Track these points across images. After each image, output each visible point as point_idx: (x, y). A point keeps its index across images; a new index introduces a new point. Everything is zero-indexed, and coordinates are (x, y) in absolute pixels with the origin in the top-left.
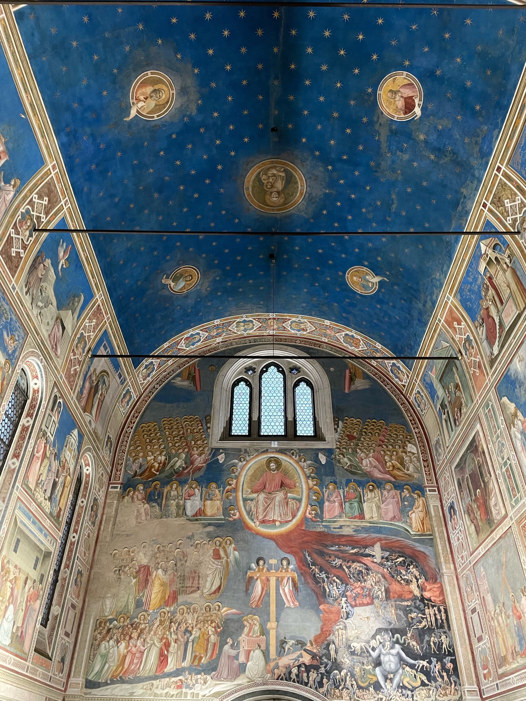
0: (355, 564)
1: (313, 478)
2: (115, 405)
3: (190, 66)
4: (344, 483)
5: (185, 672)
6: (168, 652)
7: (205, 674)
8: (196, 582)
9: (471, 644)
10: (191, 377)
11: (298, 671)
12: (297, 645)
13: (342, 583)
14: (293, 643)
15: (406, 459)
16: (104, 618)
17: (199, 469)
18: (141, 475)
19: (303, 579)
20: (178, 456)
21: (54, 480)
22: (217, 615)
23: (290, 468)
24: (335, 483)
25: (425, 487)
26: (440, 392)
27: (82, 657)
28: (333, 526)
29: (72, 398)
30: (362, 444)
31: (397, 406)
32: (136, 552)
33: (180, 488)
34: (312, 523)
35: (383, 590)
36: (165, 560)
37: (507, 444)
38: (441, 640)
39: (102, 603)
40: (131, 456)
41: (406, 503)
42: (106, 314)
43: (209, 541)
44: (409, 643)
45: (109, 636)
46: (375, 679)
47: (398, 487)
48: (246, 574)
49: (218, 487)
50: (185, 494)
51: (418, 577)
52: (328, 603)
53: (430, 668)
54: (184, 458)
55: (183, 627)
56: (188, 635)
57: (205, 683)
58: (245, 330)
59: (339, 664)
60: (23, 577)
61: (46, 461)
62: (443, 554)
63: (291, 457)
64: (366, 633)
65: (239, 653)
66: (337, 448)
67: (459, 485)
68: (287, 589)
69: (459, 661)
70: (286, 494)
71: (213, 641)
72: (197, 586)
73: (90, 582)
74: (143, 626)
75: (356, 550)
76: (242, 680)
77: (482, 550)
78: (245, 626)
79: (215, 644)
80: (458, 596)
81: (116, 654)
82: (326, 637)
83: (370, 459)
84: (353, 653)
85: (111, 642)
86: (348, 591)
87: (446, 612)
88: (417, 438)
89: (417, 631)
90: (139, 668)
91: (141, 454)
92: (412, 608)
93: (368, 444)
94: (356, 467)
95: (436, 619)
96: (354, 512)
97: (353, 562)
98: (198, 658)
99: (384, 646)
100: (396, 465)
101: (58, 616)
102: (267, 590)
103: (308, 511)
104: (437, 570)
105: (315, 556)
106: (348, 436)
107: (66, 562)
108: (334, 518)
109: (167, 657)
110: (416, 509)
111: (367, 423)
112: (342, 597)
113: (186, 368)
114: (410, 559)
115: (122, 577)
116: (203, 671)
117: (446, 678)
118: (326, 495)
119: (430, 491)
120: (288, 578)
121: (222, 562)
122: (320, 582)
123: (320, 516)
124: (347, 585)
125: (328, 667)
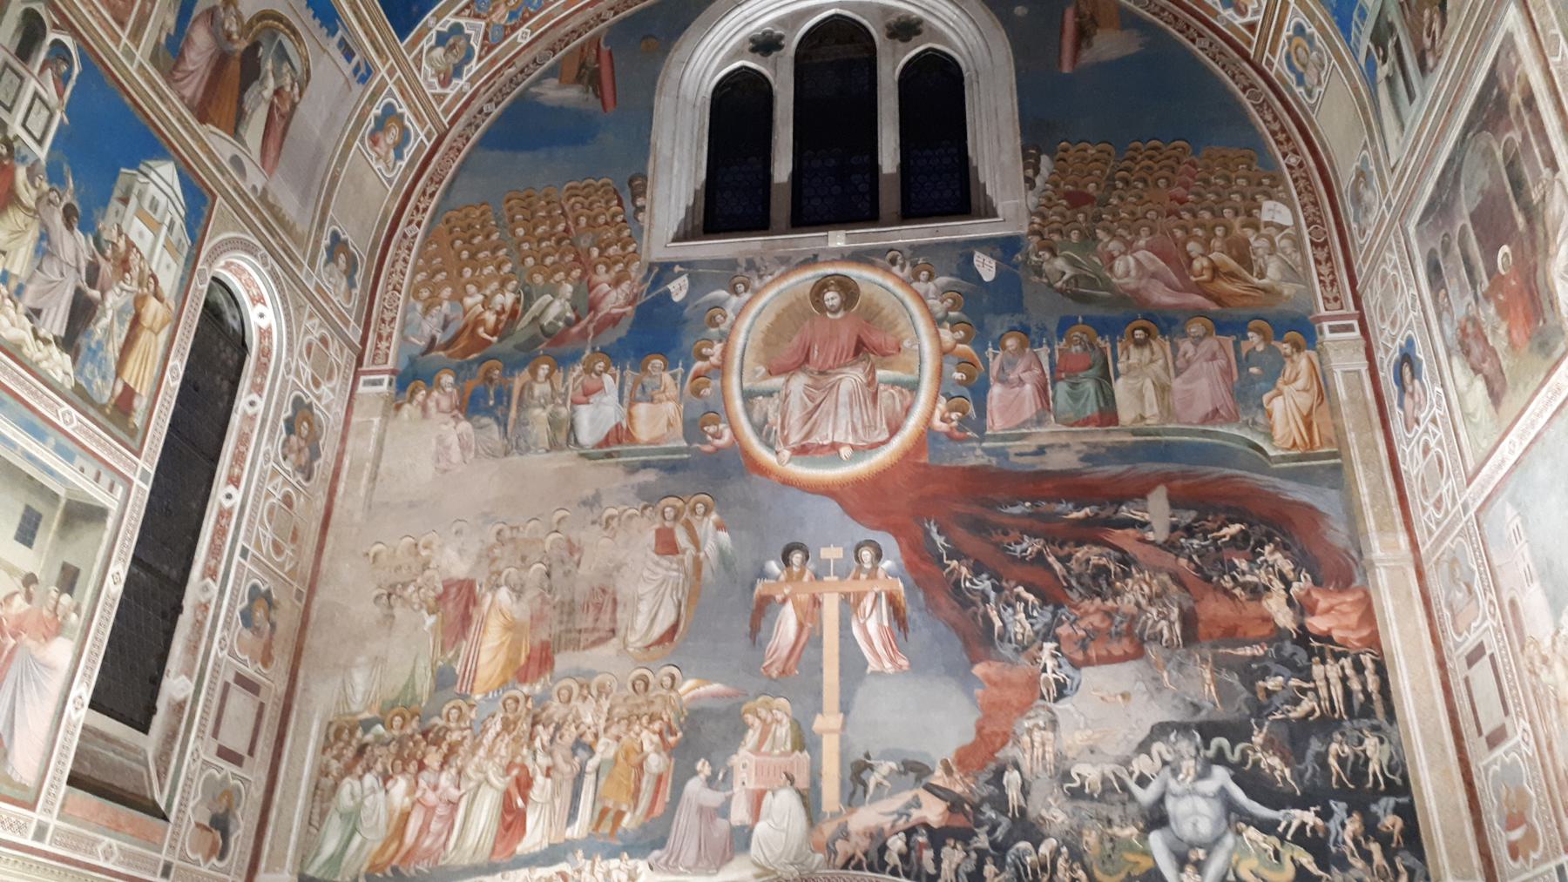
0: (1086, 548)
1: (954, 324)
2: (348, 146)
4: (1053, 327)
5: (574, 852)
6: (525, 799)
7: (631, 857)
8: (605, 618)
10: (587, 73)
11: (907, 844)
12: (905, 773)
13: (1044, 602)
14: (892, 770)
15: (1258, 244)
16: (348, 718)
17: (614, 320)
18: (448, 345)
19: (921, 595)
21: (78, 292)
23: (883, 302)
24: (1025, 330)
25: (1320, 319)
27: (291, 819)
28: (1017, 451)
31: (1232, 95)
32: (434, 547)
34: (952, 444)
35: (1175, 613)
36: (519, 563)
38: (1364, 751)
39: (343, 681)
40: (417, 298)
41: (1254, 370)
43: (645, 508)
44: (1256, 763)
45: (363, 763)
46: (1146, 864)
47: (1228, 326)
48: (753, 586)
49: (670, 365)
50: (574, 390)
51: (1291, 576)
52: (1001, 658)
53: (1327, 831)
54: (569, 295)
55: (570, 734)
56: (582, 754)
59: (1033, 825)
62: (1373, 506)
63: (887, 271)
64: (1120, 737)
65: (729, 799)
67: (1434, 271)
68: (873, 625)
69: (1424, 809)
70: (873, 371)
71: (655, 770)
72: (607, 627)
73: (311, 627)
74: (455, 736)
75: (1087, 510)
77: (1509, 451)
78: (746, 727)
79: (660, 779)
80: (1422, 622)
81: (382, 810)
82: (992, 754)
83: (1140, 255)
85: (369, 779)
86: (1061, 622)
87: (1381, 670)
88: (1295, 181)
89: (1284, 730)
90: (445, 845)
91: (447, 292)
92: (1270, 664)
93: (1132, 213)
94: (1092, 282)
95: (1348, 693)
96: (1084, 406)
98: (611, 814)
99: (1175, 772)
100: (1226, 264)
101: (185, 701)
102: (812, 630)
103: (937, 414)
104: (1354, 554)
105: (961, 534)
106: (1067, 196)
107: (207, 561)
108: (1018, 427)
109: (521, 816)
110: (1286, 383)
111: (1131, 153)
112: (1045, 639)
114: (1264, 528)
115: (398, 612)
116: (626, 848)
118: (994, 367)
119: (1333, 330)
120: (878, 596)
121: (683, 561)
122: (973, 603)
123: (975, 422)
124: (1058, 606)
125: (1000, 834)
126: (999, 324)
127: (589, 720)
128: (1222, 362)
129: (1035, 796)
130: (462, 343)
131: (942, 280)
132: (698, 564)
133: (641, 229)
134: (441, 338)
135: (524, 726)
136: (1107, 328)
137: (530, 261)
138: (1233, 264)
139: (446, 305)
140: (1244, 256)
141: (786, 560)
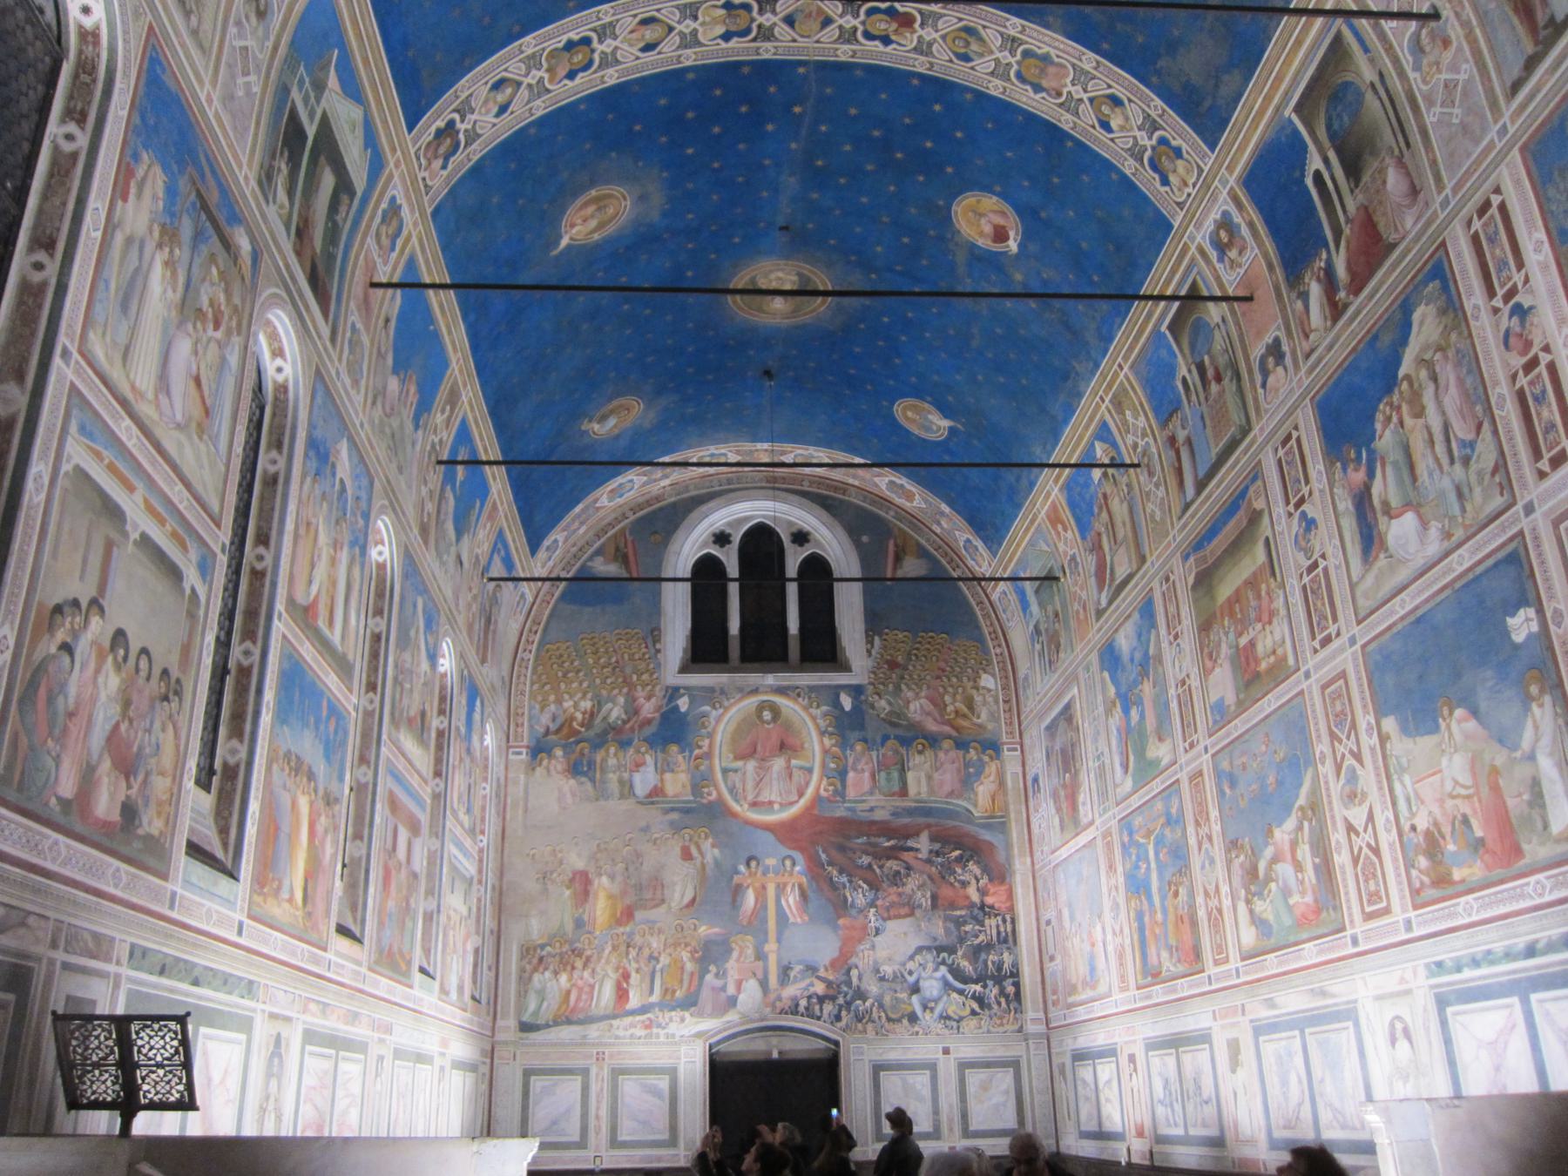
1: (831, 734)
4: (879, 740)
8: (659, 892)
10: (624, 559)
15: (978, 699)
17: (649, 722)
18: (558, 731)
20: (613, 700)
24: (865, 741)
26: (1034, 608)
29: (473, 658)
33: (621, 754)
37: (1103, 736)
46: (909, 1009)
47: (961, 745)
49: (682, 751)
55: (646, 952)
57: (683, 1020)
68: (791, 900)
70: (789, 761)
74: (588, 953)
76: (732, 1016)
79: (692, 974)
85: (548, 974)
87: (1013, 921)
94: (899, 716)
95: (999, 933)
97: (888, 858)
105: (834, 853)
106: (887, 662)
109: (626, 992)
115: (550, 887)
117: (1004, 1005)
118: (850, 760)
123: (841, 793)
126: (855, 735)
127: (655, 945)
129: (864, 979)
130: (565, 731)
131: (825, 708)
132: (703, 866)
133: (659, 665)
134: (553, 727)
135: (623, 948)
136: (906, 742)
137: (598, 681)
138: (965, 710)
139: (553, 707)
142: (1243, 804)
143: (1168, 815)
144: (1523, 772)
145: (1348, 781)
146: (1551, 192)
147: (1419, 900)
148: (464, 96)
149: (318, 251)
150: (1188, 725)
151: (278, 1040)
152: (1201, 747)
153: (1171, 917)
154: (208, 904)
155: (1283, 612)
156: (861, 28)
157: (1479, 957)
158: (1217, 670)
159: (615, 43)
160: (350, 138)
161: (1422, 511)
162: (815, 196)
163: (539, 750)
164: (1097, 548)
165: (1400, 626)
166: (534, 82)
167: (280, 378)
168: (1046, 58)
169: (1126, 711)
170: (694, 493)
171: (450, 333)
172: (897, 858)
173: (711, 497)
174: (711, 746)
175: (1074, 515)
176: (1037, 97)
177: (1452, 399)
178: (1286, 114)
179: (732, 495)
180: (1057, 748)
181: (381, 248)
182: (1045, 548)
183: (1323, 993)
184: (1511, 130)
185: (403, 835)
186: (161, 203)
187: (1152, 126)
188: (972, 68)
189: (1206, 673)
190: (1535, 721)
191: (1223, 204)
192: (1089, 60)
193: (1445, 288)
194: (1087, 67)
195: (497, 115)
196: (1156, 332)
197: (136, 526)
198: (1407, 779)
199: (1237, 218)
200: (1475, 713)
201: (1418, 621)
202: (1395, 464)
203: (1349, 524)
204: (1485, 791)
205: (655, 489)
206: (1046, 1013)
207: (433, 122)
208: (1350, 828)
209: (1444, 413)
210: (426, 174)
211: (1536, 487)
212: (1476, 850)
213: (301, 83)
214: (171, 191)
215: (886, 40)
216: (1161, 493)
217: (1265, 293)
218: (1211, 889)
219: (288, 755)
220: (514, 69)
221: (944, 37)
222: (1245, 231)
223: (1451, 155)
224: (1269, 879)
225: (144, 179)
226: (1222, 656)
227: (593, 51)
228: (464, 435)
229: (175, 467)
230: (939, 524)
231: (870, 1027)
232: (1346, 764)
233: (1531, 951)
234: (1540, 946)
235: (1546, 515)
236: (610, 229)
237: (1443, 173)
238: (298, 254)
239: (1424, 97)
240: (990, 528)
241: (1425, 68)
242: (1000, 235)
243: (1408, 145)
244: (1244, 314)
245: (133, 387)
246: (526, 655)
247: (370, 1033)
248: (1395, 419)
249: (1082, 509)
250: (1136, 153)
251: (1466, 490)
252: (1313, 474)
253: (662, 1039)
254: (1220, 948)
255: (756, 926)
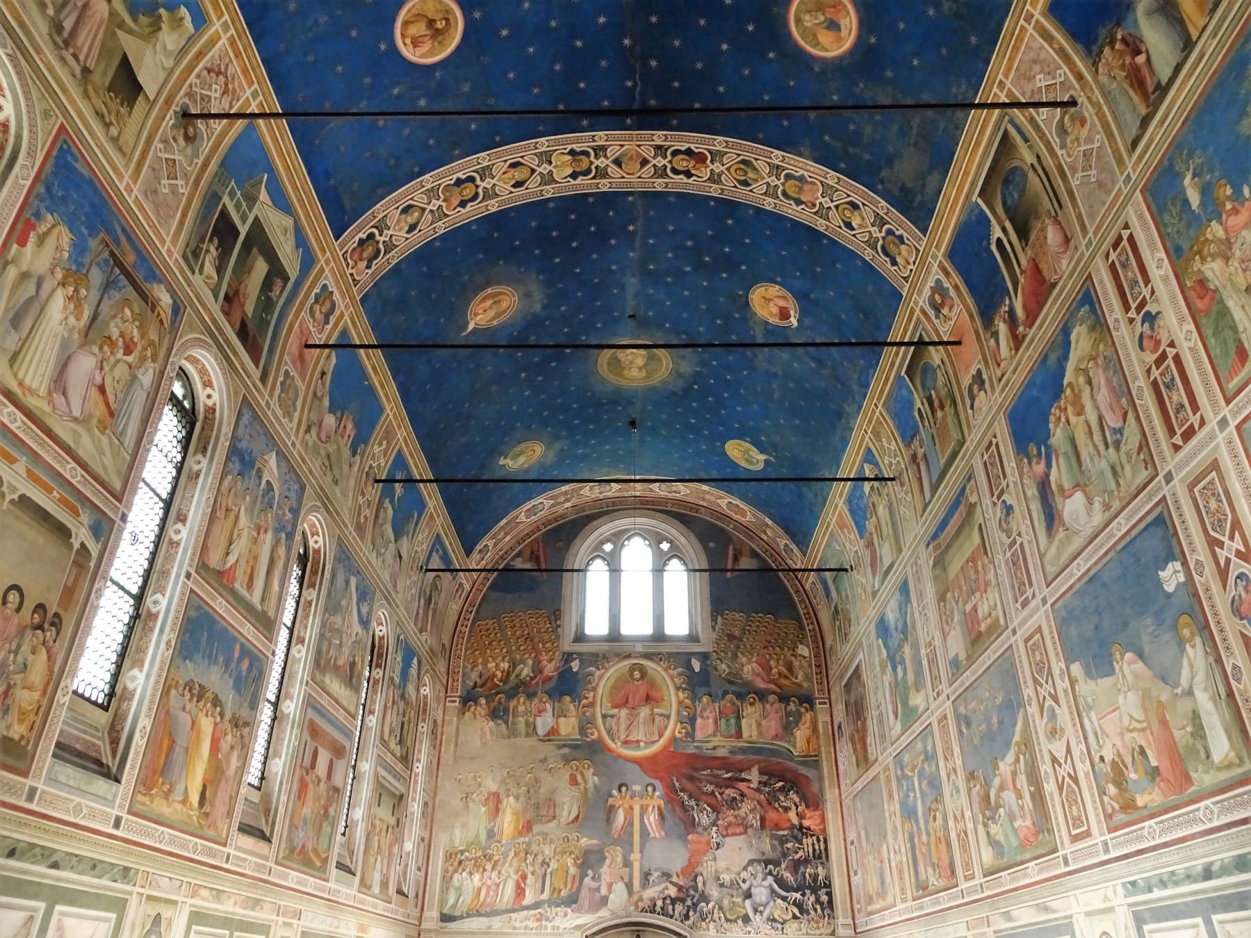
1: (684, 689)
3: (534, 276)
4: (720, 694)
8: (551, 810)
9: (849, 876)
10: (534, 557)
13: (714, 811)
15: (796, 663)
17: (550, 678)
18: (483, 685)
20: (523, 662)
22: (576, 847)
24: (710, 695)
29: (411, 628)
30: (745, 646)
31: (790, 594)
33: (528, 703)
35: (758, 817)
42: (438, 516)
45: (461, 868)
46: (744, 912)
47: (784, 699)
48: (607, 801)
52: (699, 833)
55: (540, 859)
56: (545, 866)
57: (566, 915)
58: (601, 493)
60: (385, 827)
61: (395, 706)
63: (659, 664)
66: (716, 652)
68: (652, 818)
74: (496, 858)
76: (604, 913)
77: (859, 785)
78: (606, 858)
84: (722, 885)
89: (792, 863)
91: (480, 660)
95: (814, 850)
97: (727, 788)
109: (524, 890)
113: (526, 545)
115: (470, 804)
117: (819, 911)
118: (699, 709)
119: (820, 703)
123: (691, 735)
124: (718, 813)
125: (695, 900)
126: (702, 690)
127: (547, 853)
128: (779, 714)
129: (707, 885)
131: (680, 670)
132: (585, 789)
135: (523, 855)
136: (741, 696)
137: (514, 648)
138: (786, 672)
139: (480, 666)
140: (790, 667)
141: (620, 790)
142: (976, 742)
143: (925, 751)
144: (1184, 706)
145: (1050, 719)
146: (1166, 218)
147: (1112, 825)
148: (380, 216)
149: (250, 315)
150: (936, 679)
151: (158, 919)
152: (944, 696)
153: (933, 838)
154: (77, 799)
155: (994, 582)
156: (669, 166)
157: (1165, 878)
158: (953, 632)
159: (494, 181)
160: (283, 239)
161: (1087, 489)
162: (651, 291)
163: (468, 699)
164: (870, 545)
165: (1078, 586)
166: (435, 209)
167: (210, 403)
168: (801, 179)
169: (894, 669)
170: (588, 513)
171: (383, 387)
172: (734, 788)
173: (601, 515)
174: (594, 696)
175: (854, 519)
176: (799, 208)
177: (1103, 396)
178: (974, 199)
179: (617, 513)
180: (852, 701)
181: (314, 320)
182: (837, 547)
183: (1046, 909)
184: (1134, 178)
185: (324, 758)
186: (66, 255)
187: (880, 222)
188: (751, 191)
189: (945, 635)
190: (1189, 660)
191: (935, 274)
192: (832, 177)
193: (1093, 310)
194: (831, 183)
195: (408, 232)
196: (898, 375)
197: (13, 489)
198: (1093, 715)
199: (947, 285)
200: (1141, 655)
201: (1091, 580)
202: (1066, 454)
203: (1036, 506)
204: (1155, 725)
205: (560, 510)
206: (853, 919)
207: (354, 234)
208: (1054, 760)
209: (1098, 409)
210: (353, 271)
211: (1173, 458)
212: (1153, 779)
213: (232, 194)
214: (79, 248)
215: (688, 174)
216: (909, 498)
217: (969, 339)
218: (958, 814)
219: (189, 685)
220: (419, 199)
221: (728, 169)
222: (952, 293)
223: (1091, 207)
224: (998, 806)
225: (46, 235)
226: (955, 621)
227: (477, 187)
228: (400, 461)
229: (68, 450)
230: (766, 533)
231: (712, 924)
232: (1047, 705)
233: (1208, 874)
234: (1215, 868)
235: (1181, 481)
236: (503, 318)
237: (1086, 222)
238: (226, 314)
239: (1069, 167)
240: (800, 534)
241: (1069, 145)
242: (784, 314)
243: (1061, 207)
244: (955, 355)
245: (21, 384)
246: (463, 629)
247: (275, 918)
248: (1063, 419)
249: (859, 512)
250: (872, 243)
251: (1118, 468)
252: (1008, 470)
253: (549, 930)
254: (968, 866)
255: (625, 839)
